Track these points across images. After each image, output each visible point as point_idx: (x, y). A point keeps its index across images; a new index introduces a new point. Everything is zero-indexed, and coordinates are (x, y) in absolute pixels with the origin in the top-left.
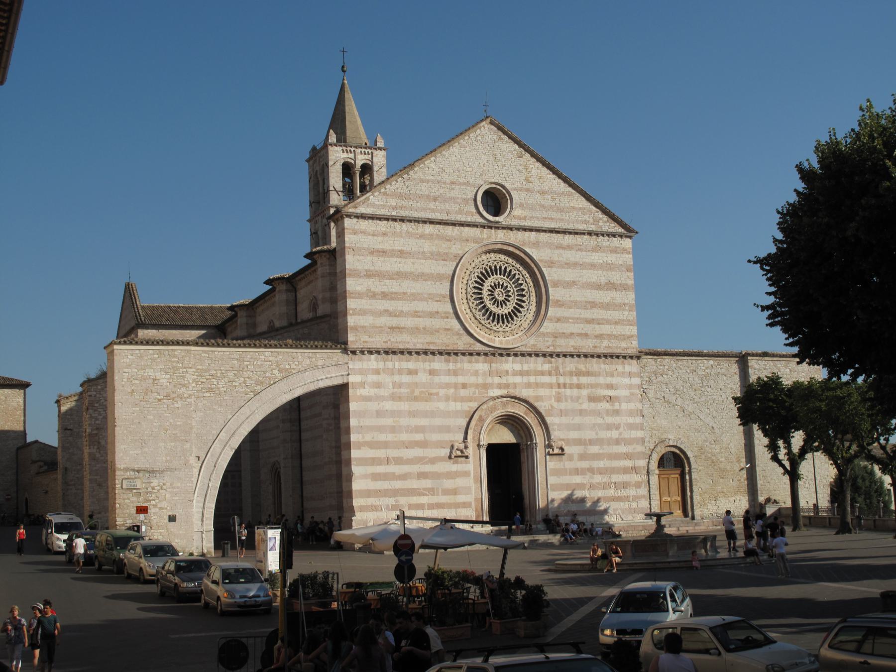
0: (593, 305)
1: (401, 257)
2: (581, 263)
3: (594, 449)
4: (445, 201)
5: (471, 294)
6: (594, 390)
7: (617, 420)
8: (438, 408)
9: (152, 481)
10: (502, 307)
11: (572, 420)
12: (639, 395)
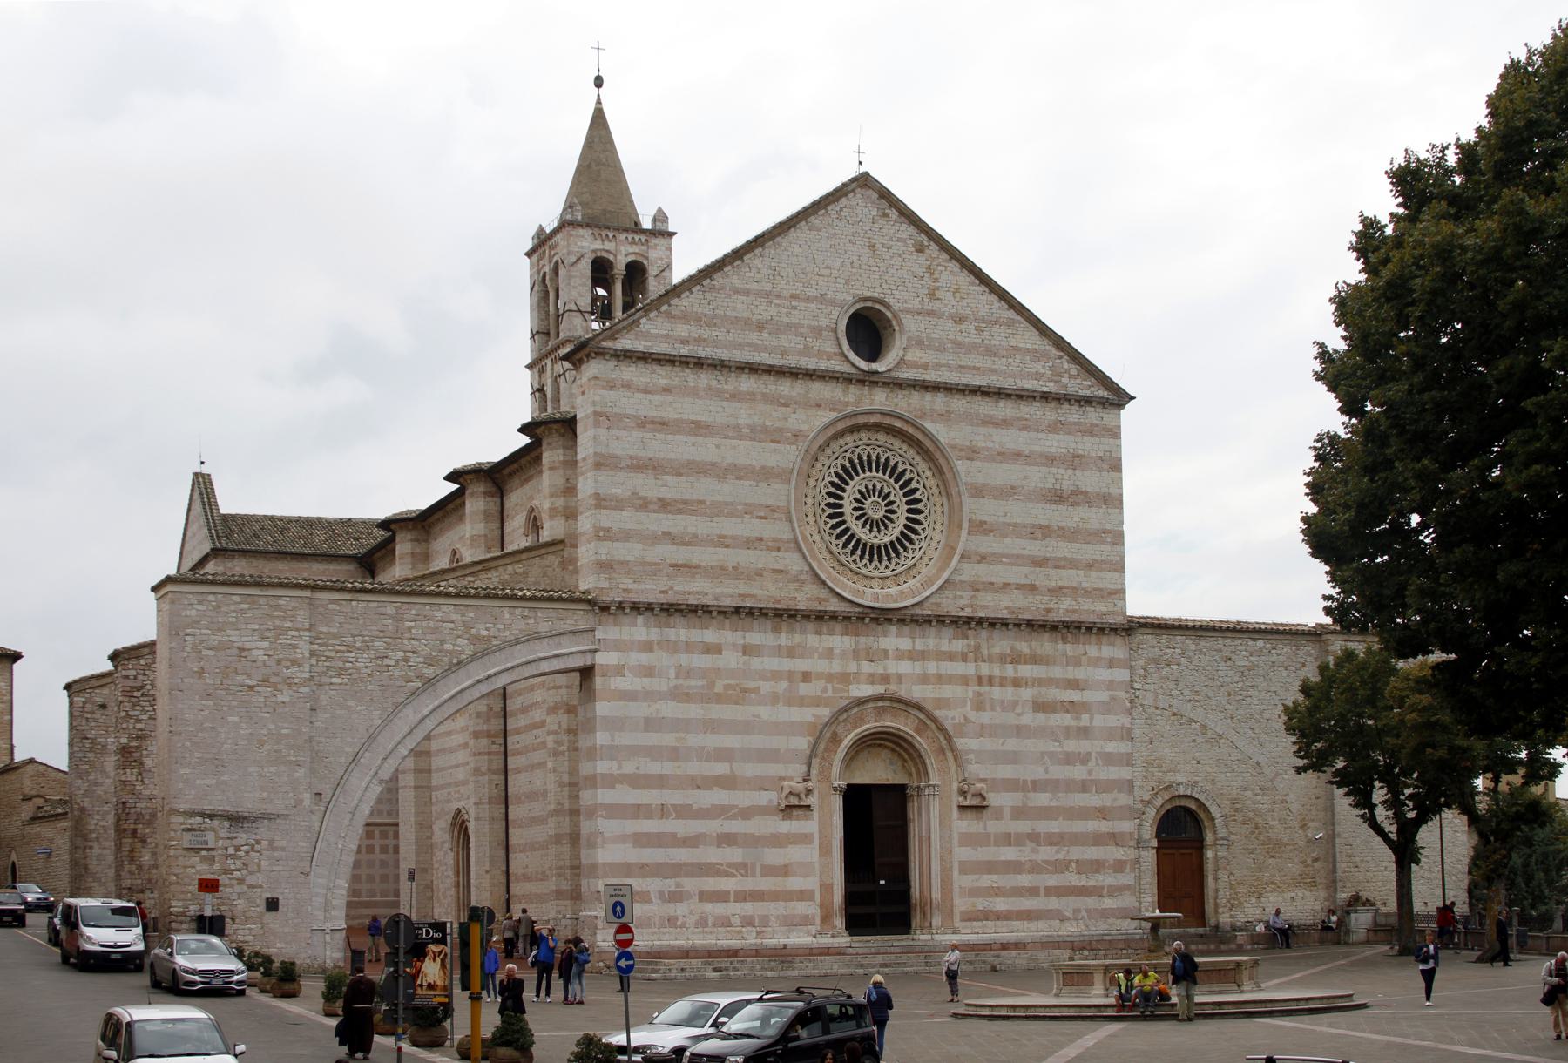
0: (1045, 531)
1: (696, 435)
2: (1027, 452)
3: (1042, 799)
4: (778, 331)
5: (823, 506)
6: (1043, 690)
7: (1083, 746)
8: (758, 716)
9: (235, 835)
10: (879, 531)
11: (1003, 744)
12: (1127, 702)
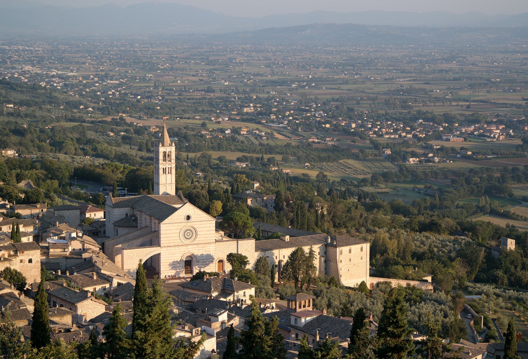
0: (206, 234)
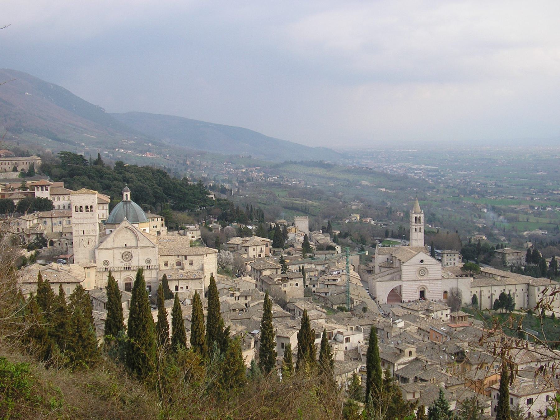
0: (435, 273)
